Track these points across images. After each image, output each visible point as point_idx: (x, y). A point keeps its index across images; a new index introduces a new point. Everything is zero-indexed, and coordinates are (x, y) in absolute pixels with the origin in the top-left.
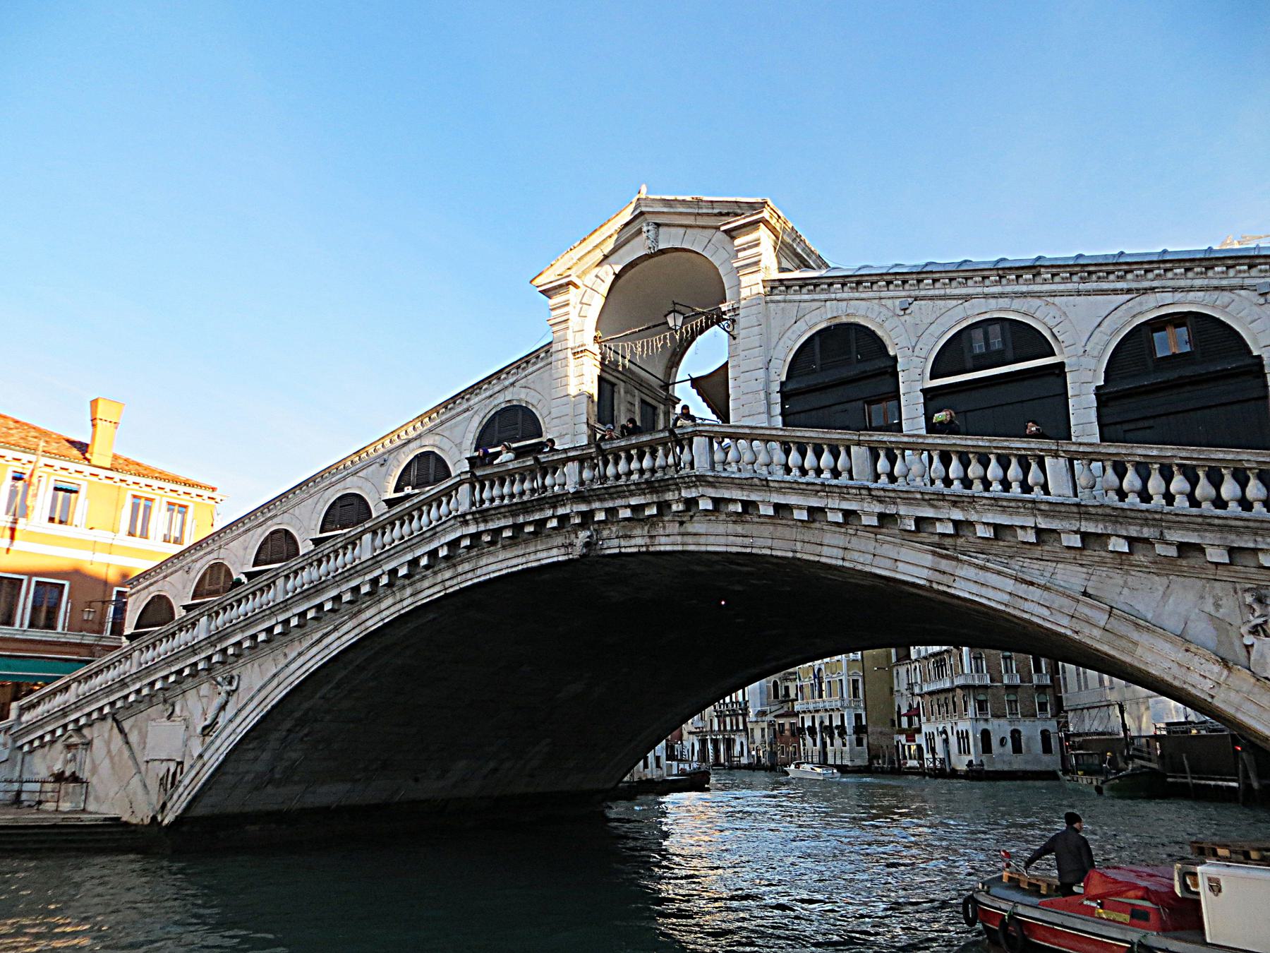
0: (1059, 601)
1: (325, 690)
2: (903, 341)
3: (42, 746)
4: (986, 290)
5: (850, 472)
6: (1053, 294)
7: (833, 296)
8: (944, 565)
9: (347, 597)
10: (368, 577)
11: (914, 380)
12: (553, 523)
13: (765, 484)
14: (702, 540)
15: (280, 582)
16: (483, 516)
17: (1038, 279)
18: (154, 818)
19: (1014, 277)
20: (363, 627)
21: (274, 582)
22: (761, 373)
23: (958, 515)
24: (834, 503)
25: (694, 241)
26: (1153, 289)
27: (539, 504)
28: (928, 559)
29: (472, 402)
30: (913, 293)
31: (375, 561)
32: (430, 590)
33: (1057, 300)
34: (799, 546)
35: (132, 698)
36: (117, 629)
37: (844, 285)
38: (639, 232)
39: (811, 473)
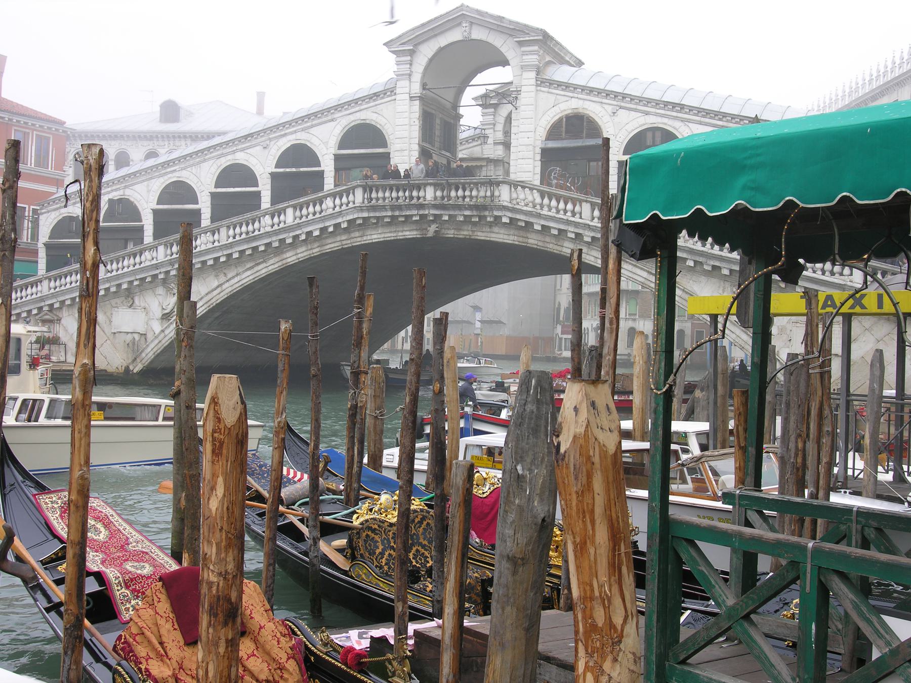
5: (581, 213)
6: (689, 121)
7: (576, 95)
10: (292, 234)
12: (418, 218)
13: (539, 216)
14: (501, 236)
15: (223, 231)
16: (374, 208)
18: (127, 369)
20: (284, 262)
21: (219, 230)
24: (571, 229)
25: (496, 40)
27: (409, 207)
29: (336, 116)
30: (619, 103)
32: (332, 245)
33: (690, 125)
34: (551, 246)
38: (460, 24)
39: (562, 212)
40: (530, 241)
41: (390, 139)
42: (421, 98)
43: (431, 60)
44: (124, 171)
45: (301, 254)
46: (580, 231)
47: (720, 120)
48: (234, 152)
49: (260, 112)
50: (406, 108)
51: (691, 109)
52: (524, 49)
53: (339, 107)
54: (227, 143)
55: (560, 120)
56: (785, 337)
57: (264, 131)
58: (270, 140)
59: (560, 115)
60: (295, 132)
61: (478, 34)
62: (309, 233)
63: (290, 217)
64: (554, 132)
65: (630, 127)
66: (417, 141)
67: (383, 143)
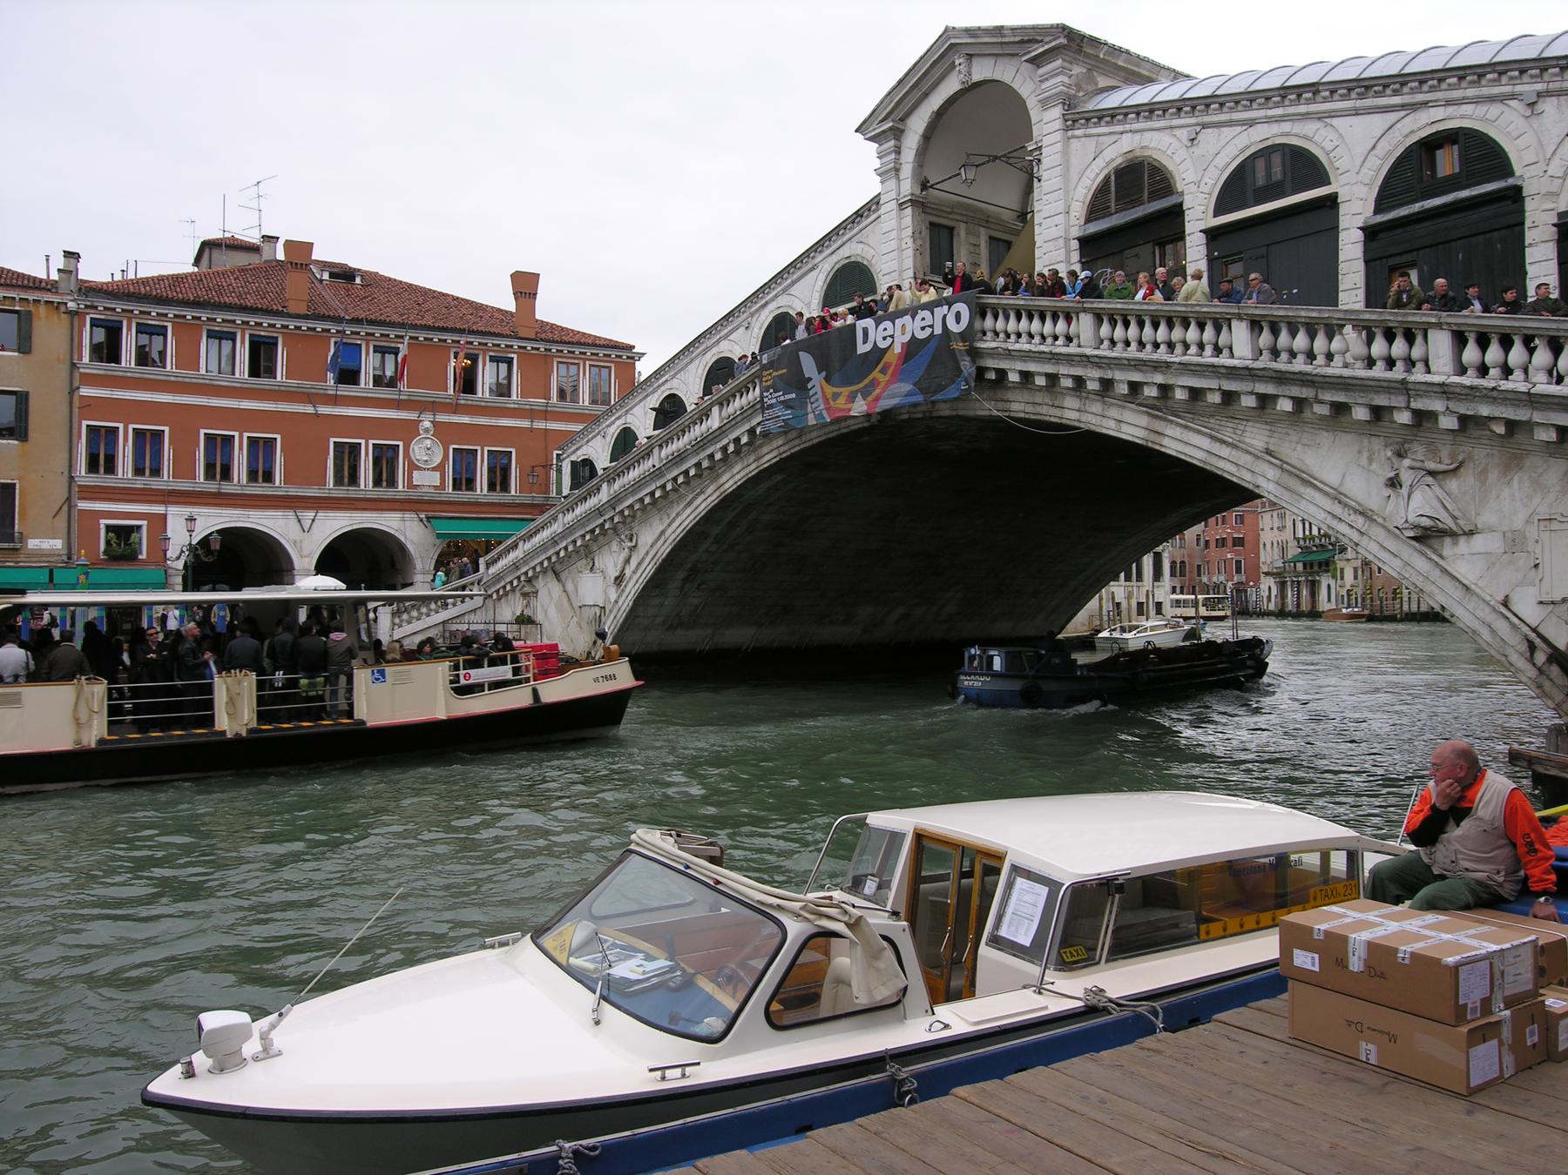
0: (1245, 459)
1: (705, 546)
3: (506, 594)
4: (1271, 113)
7: (1128, 127)
8: (1158, 426)
9: (705, 464)
10: (719, 445)
13: (1009, 354)
17: (1319, 98)
19: (1293, 97)
22: (1060, 219)
23: (1159, 379)
24: (1063, 370)
26: (1425, 104)
28: (1143, 420)
33: (1335, 122)
34: (1044, 410)
35: (562, 554)
36: (559, 491)
37: (1138, 114)
38: (953, 66)
40: (1014, 406)
42: (914, 202)
43: (927, 137)
46: (1079, 372)
47: (1396, 93)
48: (718, 342)
50: (893, 224)
52: (1042, 71)
55: (1107, 180)
56: (1523, 561)
58: (752, 315)
59: (1106, 172)
60: (776, 296)
61: (982, 71)
62: (737, 440)
65: (1221, 160)
66: (910, 273)
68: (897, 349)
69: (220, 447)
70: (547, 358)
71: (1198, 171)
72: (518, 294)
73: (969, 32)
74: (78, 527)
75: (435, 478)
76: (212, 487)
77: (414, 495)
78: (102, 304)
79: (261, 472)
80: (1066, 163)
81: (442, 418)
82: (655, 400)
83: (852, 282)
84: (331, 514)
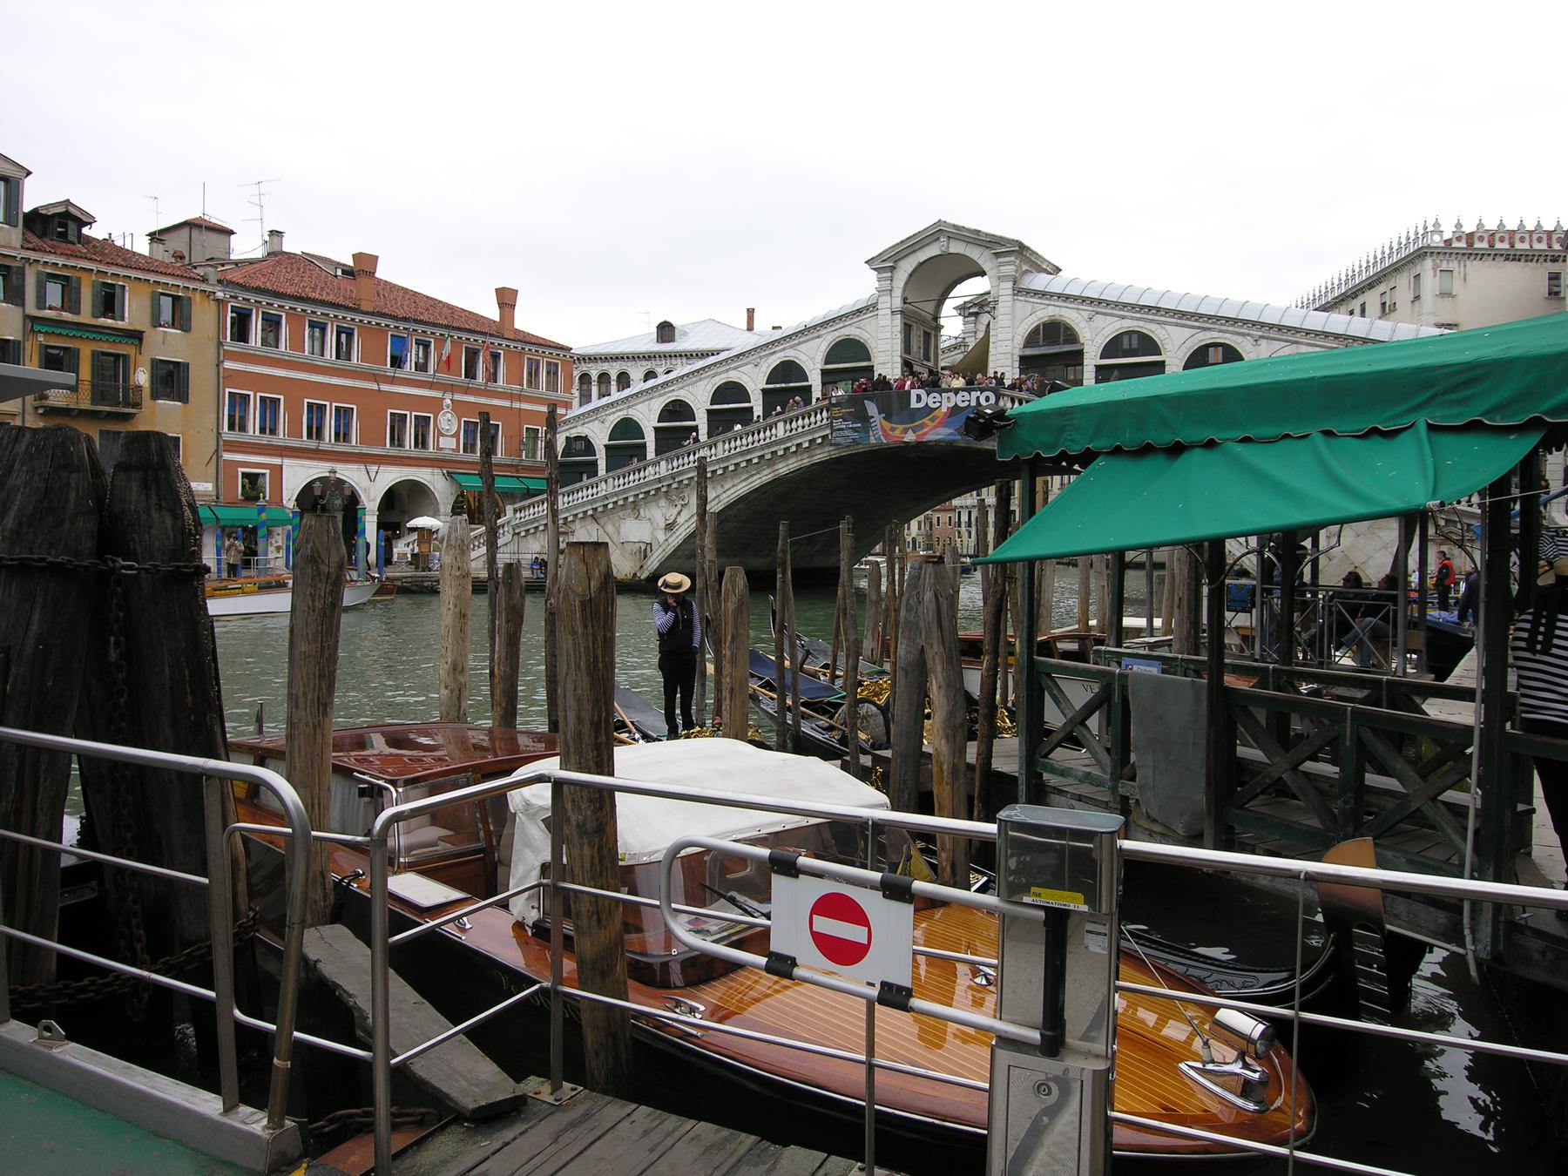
2: (1088, 336)
6: (1165, 323)
11: (1092, 359)
15: (720, 445)
25: (974, 253)
31: (789, 439)
41: (873, 352)
44: (627, 392)
45: (793, 464)
49: (750, 328)
50: (888, 322)
51: (1167, 311)
53: (824, 324)
54: (720, 362)
55: (1038, 327)
57: (755, 349)
61: (956, 248)
62: (799, 445)
63: (780, 431)
64: (1031, 340)
67: (869, 359)
68: (944, 409)
69: (317, 411)
70: (521, 354)
71: (1093, 336)
72: (501, 305)
73: (955, 226)
74: (222, 472)
75: (452, 443)
76: (313, 444)
77: (440, 455)
78: (242, 295)
79: (342, 435)
80: (1013, 313)
81: (458, 397)
82: (658, 404)
83: (849, 349)
84: (389, 468)
